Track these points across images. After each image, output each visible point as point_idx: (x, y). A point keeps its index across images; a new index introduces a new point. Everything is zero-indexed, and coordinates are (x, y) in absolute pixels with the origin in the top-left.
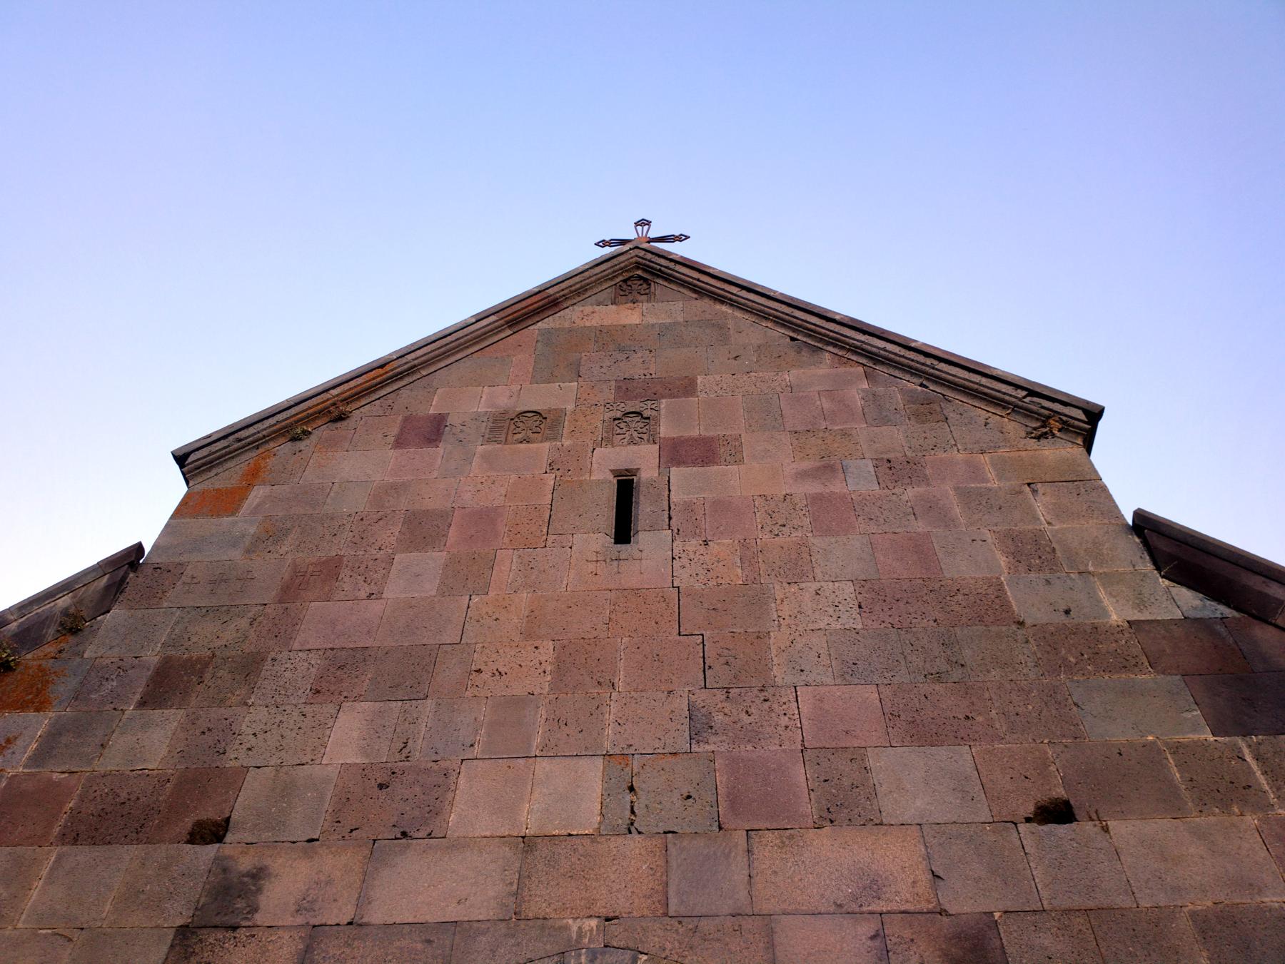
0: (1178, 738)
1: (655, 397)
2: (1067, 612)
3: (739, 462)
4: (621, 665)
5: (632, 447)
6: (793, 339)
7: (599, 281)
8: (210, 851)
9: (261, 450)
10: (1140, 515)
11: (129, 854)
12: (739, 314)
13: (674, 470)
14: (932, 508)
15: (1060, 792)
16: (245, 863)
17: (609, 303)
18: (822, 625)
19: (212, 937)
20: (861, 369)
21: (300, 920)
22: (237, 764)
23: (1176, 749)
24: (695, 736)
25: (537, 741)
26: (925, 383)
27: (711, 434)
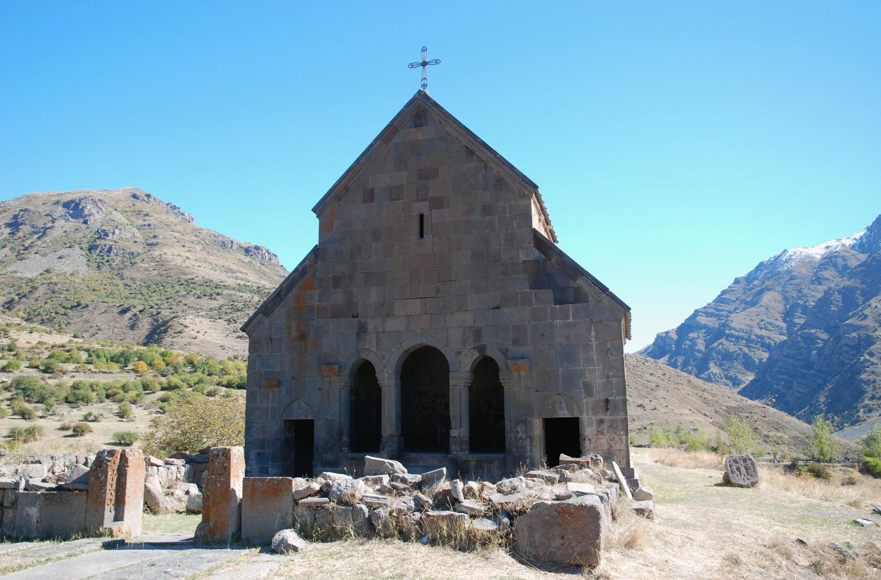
8: (357, 319)
16: (363, 321)
20: (483, 164)
24: (437, 293)
25: (408, 295)
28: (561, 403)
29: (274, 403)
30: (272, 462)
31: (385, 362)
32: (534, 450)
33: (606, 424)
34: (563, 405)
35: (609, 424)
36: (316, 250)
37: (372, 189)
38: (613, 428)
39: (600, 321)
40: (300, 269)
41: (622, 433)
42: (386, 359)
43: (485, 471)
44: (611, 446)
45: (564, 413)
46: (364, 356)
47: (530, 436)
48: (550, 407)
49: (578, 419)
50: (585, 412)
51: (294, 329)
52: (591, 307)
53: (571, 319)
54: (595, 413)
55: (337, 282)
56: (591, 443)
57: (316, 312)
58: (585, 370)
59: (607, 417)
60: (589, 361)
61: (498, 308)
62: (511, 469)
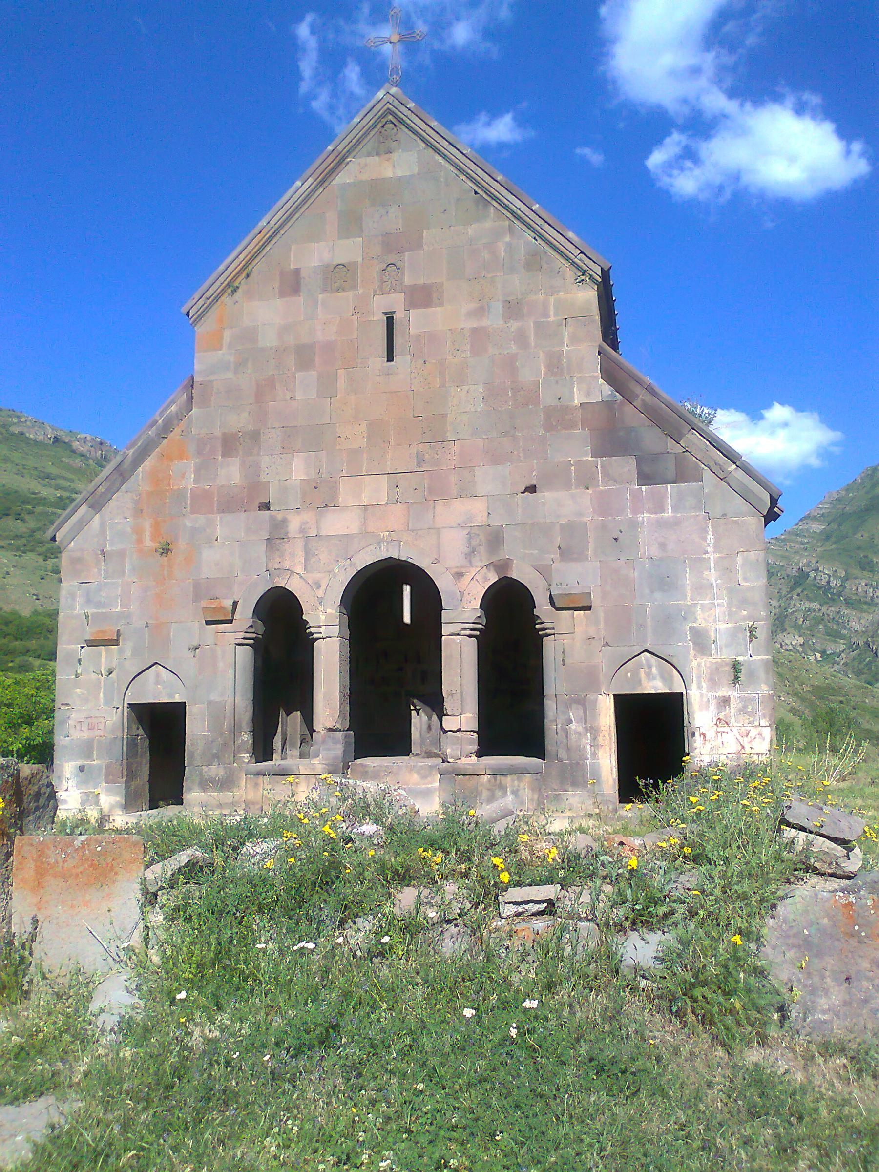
2: (560, 399)
3: (441, 304)
4: (392, 432)
6: (476, 193)
7: (366, 134)
9: (219, 302)
11: (243, 515)
12: (448, 165)
14: (521, 338)
15: (534, 482)
16: (280, 516)
17: (375, 154)
18: (468, 410)
19: (278, 541)
20: (507, 223)
21: (301, 536)
22: (264, 480)
23: (577, 463)
26: (537, 238)
28: (650, 667)
31: (320, 593)
32: (600, 753)
33: (735, 705)
34: (654, 670)
37: (297, 272)
40: (160, 421)
41: (763, 722)
42: (323, 587)
44: (743, 747)
45: (654, 685)
47: (592, 727)
48: (629, 675)
52: (706, 491)
53: (669, 513)
54: (714, 683)
57: (189, 502)
59: (734, 694)
60: (702, 588)
61: (532, 489)
62: (555, 790)
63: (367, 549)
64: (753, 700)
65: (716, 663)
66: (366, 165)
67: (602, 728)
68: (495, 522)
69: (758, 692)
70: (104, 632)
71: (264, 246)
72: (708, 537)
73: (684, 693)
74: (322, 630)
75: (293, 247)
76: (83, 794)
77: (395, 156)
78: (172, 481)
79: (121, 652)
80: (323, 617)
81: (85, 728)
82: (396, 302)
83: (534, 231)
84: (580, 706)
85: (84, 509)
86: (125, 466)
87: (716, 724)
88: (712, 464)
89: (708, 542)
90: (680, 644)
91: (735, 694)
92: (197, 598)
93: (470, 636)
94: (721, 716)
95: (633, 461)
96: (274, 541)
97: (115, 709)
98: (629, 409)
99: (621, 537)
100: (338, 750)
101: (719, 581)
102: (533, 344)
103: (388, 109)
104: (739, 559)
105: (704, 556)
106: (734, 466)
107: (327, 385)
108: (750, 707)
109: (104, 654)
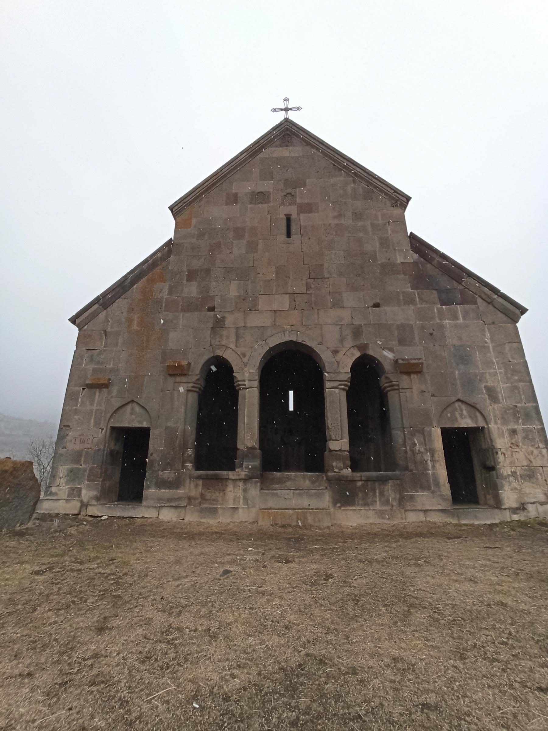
0: (404, 290)
1: (295, 188)
2: (389, 260)
3: (318, 212)
5: (290, 207)
6: (334, 165)
10: (411, 233)
11: (197, 314)
13: (301, 215)
15: (378, 301)
19: (218, 329)
20: (352, 178)
21: (234, 326)
26: (369, 185)
27: (310, 202)
28: (461, 410)
29: (101, 406)
30: (88, 481)
31: (245, 360)
32: (437, 466)
34: (465, 412)
35: (524, 435)
36: (169, 243)
37: (236, 195)
38: (529, 439)
39: (493, 323)
42: (248, 357)
43: (377, 494)
44: (531, 462)
45: (466, 422)
46: (219, 353)
48: (449, 415)
49: (483, 428)
50: (493, 420)
51: (136, 322)
52: (481, 309)
53: (461, 320)
54: (505, 421)
55: (191, 276)
56: (505, 457)
57: (164, 305)
58: (485, 373)
59: (519, 427)
60: (488, 364)
61: (377, 305)
63: (276, 335)
64: (531, 431)
65: (504, 408)
66: (275, 151)
67: (437, 449)
68: (357, 322)
69: (534, 426)
70: (99, 379)
71: (217, 182)
72: (486, 334)
73: (486, 427)
74: (246, 383)
75: (234, 183)
76: (70, 489)
77: (290, 148)
78: (154, 294)
79: (109, 393)
80: (247, 375)
81: (78, 442)
82: (293, 211)
83: (367, 181)
84: (421, 435)
85: (96, 306)
86: (126, 284)
87: (511, 447)
88: (483, 295)
89: (487, 337)
90: (480, 396)
91: (520, 427)
92: (163, 360)
93: (343, 389)
94: (513, 441)
95: (435, 292)
96: (217, 328)
97: (101, 430)
98: (429, 266)
99: (435, 333)
100: (257, 463)
101: (497, 359)
102: (371, 233)
103: (287, 128)
104: (507, 347)
105: (486, 345)
106: (497, 296)
107: (252, 247)
108: (530, 435)
109: (98, 394)
